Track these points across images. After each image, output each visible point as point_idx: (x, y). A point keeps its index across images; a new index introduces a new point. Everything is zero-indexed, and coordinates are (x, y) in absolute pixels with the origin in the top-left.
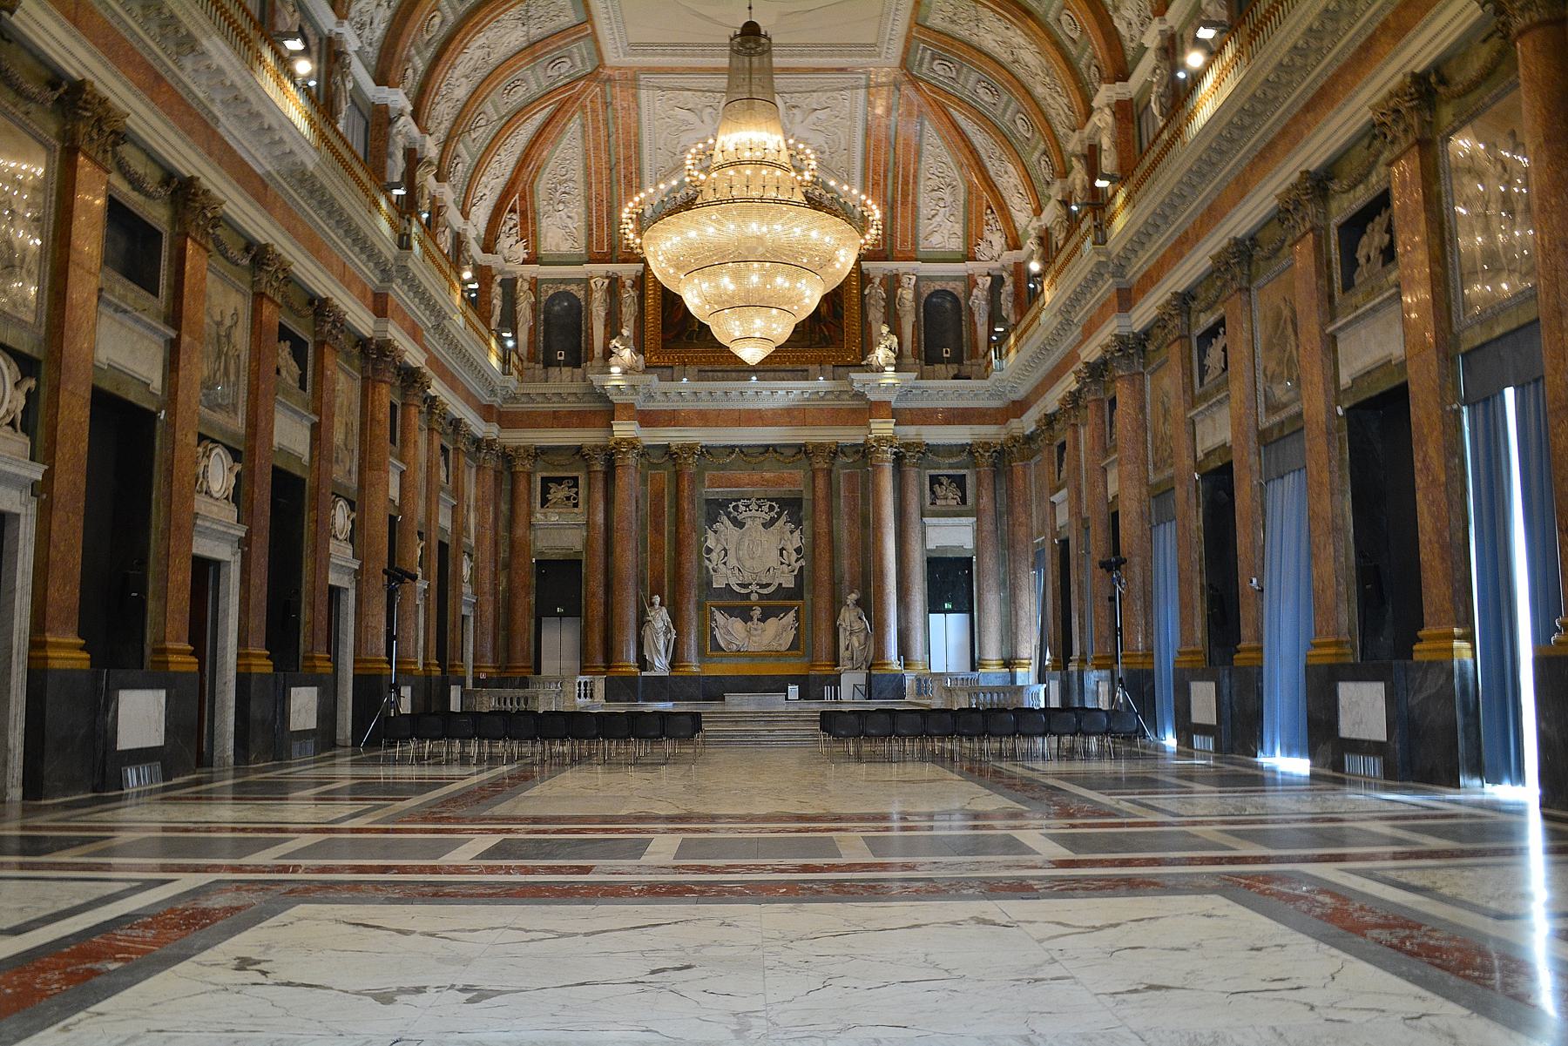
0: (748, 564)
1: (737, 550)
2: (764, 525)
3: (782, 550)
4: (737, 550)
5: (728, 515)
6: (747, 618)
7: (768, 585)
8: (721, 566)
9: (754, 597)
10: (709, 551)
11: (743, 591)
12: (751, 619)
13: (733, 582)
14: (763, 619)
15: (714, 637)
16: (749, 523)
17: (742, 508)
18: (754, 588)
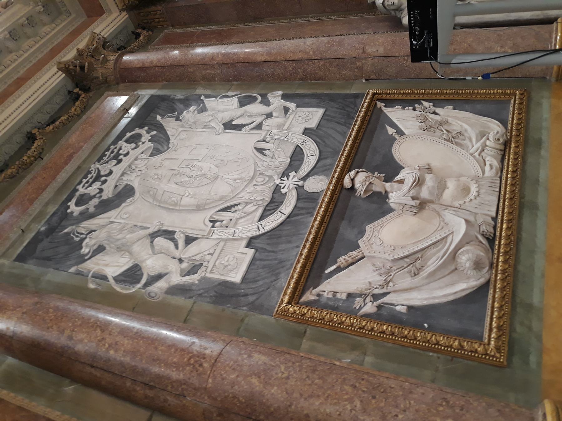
0: (222, 189)
1: (174, 208)
2: (156, 152)
3: (229, 126)
4: (174, 208)
5: (86, 216)
6: (379, 205)
7: (297, 156)
8: (193, 249)
9: (318, 184)
10: (132, 275)
11: (288, 207)
12: (383, 197)
13: (250, 227)
14: (390, 170)
15: (419, 315)
16: (133, 180)
17: (93, 190)
18: (289, 185)
